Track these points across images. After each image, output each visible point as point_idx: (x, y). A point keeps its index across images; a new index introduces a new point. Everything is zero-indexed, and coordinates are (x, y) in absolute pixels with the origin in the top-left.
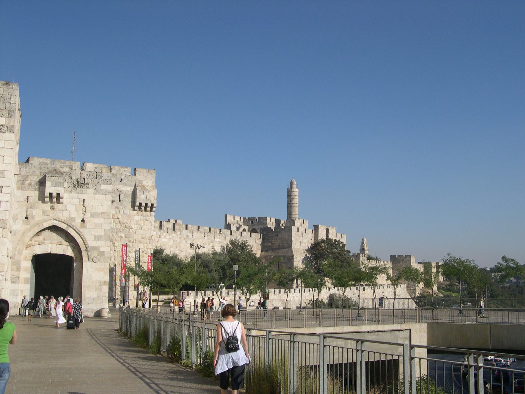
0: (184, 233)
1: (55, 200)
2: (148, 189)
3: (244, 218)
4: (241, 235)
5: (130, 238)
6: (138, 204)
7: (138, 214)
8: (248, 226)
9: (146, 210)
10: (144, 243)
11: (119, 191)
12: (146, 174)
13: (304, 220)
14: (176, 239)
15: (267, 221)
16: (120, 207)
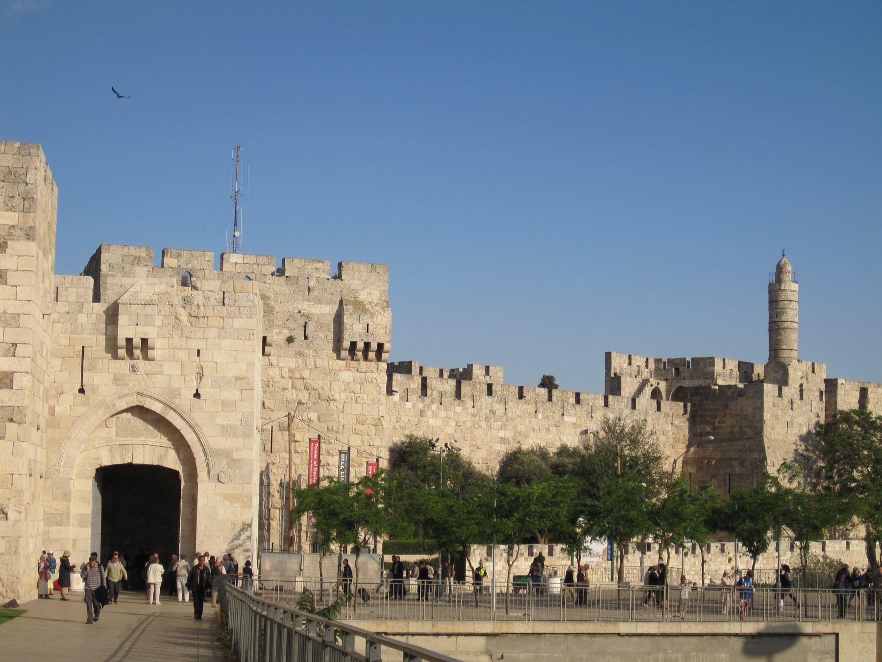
0: (484, 405)
1: (137, 352)
2: (370, 308)
3: (658, 361)
4: (634, 407)
5: (329, 424)
6: (346, 344)
7: (348, 368)
8: (666, 380)
9: (366, 358)
10: (362, 435)
11: (303, 315)
12: (365, 275)
13: (813, 364)
14: (464, 419)
15: (716, 368)
16: (306, 351)
